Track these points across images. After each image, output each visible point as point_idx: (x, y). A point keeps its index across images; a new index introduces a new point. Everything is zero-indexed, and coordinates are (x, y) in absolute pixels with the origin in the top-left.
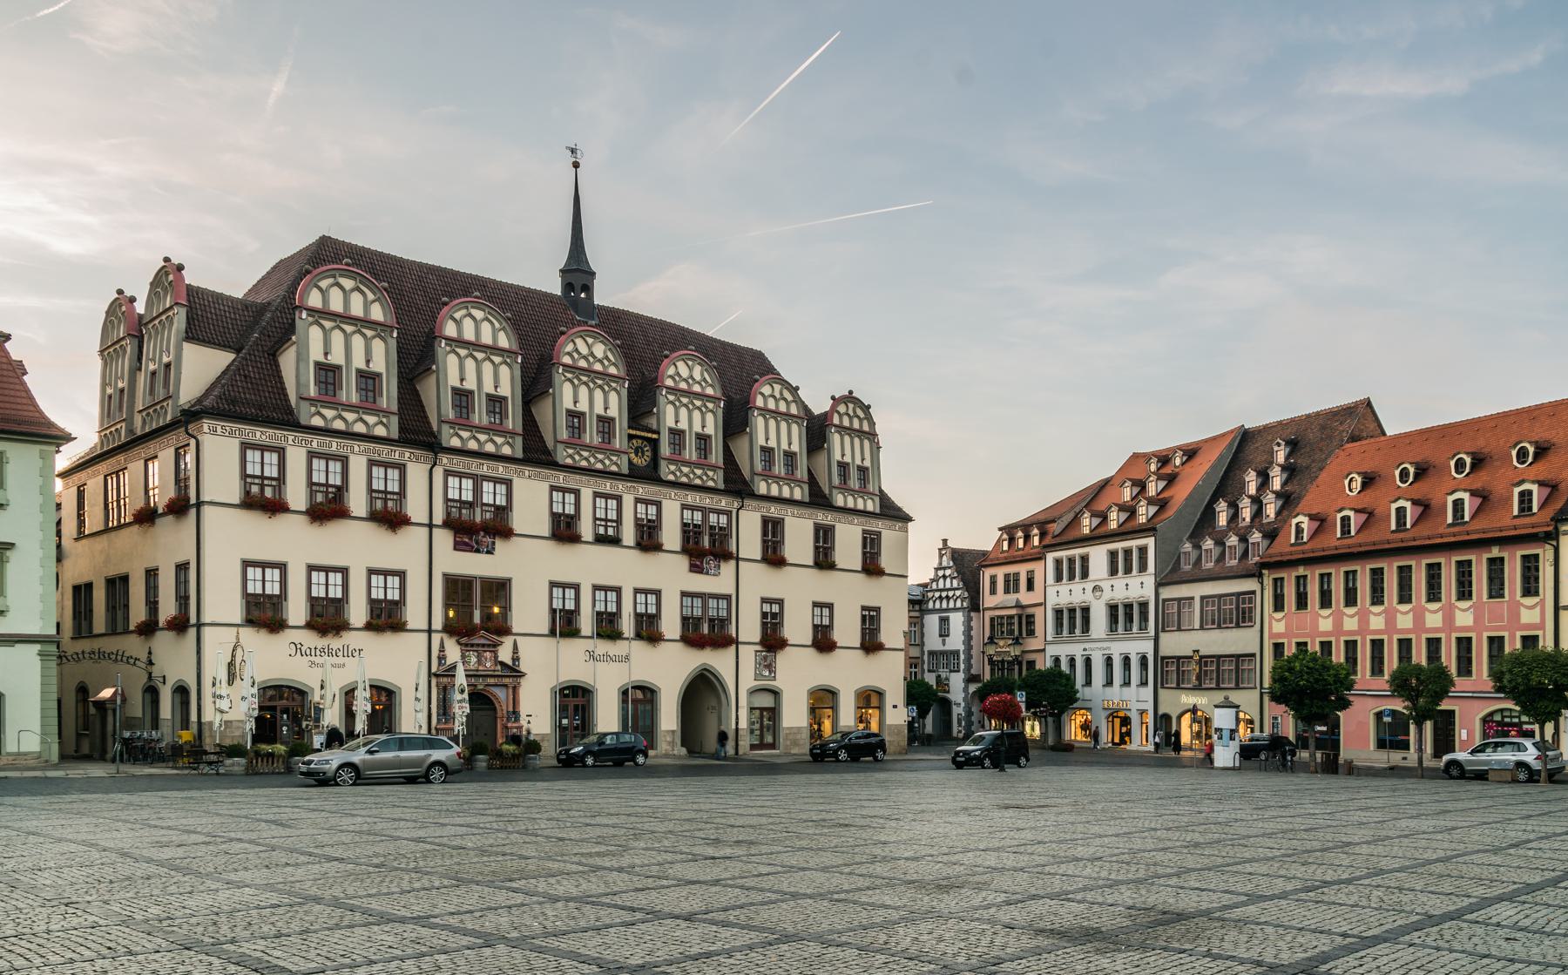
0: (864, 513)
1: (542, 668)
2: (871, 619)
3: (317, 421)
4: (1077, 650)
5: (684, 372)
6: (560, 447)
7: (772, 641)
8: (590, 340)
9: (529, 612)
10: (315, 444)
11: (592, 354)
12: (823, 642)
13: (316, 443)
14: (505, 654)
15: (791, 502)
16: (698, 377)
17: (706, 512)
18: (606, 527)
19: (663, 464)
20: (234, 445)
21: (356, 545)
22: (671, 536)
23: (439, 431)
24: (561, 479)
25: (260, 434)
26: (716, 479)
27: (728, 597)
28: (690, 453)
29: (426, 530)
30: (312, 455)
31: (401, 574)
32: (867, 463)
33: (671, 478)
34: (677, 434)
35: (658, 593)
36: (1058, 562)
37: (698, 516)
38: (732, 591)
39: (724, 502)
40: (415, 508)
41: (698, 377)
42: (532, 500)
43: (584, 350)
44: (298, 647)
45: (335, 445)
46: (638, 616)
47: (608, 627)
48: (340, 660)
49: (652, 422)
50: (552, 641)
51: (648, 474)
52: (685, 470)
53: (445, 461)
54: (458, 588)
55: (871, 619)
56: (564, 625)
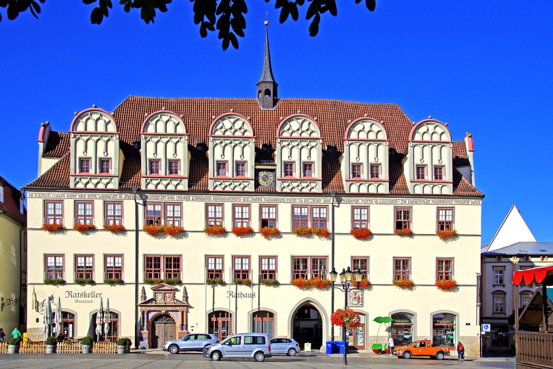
1: (201, 301)
2: (444, 266)
9: (193, 271)
18: (242, 223)
22: (284, 223)
24: (212, 199)
39: (322, 200)
40: (129, 223)
44: (70, 293)
47: (241, 277)
48: (90, 299)
50: (204, 286)
52: (295, 184)
54: (152, 262)
55: (444, 266)
56: (214, 277)
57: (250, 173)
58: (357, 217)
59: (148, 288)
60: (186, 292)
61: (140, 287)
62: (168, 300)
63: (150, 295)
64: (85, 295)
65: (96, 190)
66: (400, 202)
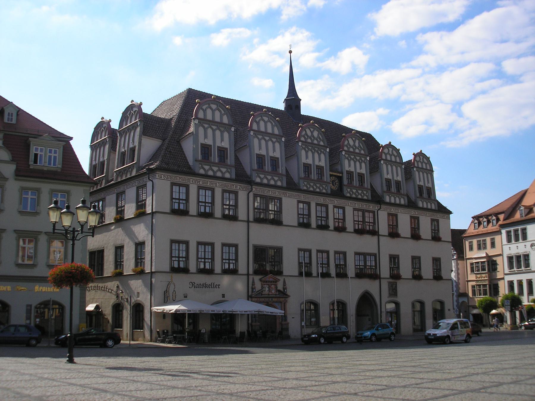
0: (431, 210)
3: (202, 172)
4: (524, 277)
5: (351, 143)
6: (301, 181)
7: (395, 276)
8: (312, 130)
10: (201, 183)
11: (313, 136)
12: (417, 277)
13: (201, 182)
14: (280, 287)
15: (400, 205)
16: (357, 145)
17: (364, 211)
19: (345, 188)
20: (168, 183)
21: (219, 232)
23: (251, 175)
24: (303, 197)
25: (180, 179)
26: (367, 195)
27: (375, 255)
28: (356, 182)
29: (246, 224)
30: (199, 188)
31: (236, 246)
32: (430, 185)
33: (348, 195)
34: (350, 173)
35: (344, 254)
36: (508, 233)
37: (360, 213)
38: (377, 252)
39: (372, 207)
41: (357, 145)
42: (290, 207)
43: (309, 133)
45: (209, 183)
46: (337, 266)
49: (339, 167)
51: (338, 193)
52: (354, 191)
53: (254, 189)
54: (260, 253)
57: (326, 177)
58: (202, 199)
59: (257, 278)
60: (284, 282)
61: (251, 278)
62: (273, 292)
63: (258, 286)
64: (205, 286)
65: (214, 177)
66: (414, 213)
